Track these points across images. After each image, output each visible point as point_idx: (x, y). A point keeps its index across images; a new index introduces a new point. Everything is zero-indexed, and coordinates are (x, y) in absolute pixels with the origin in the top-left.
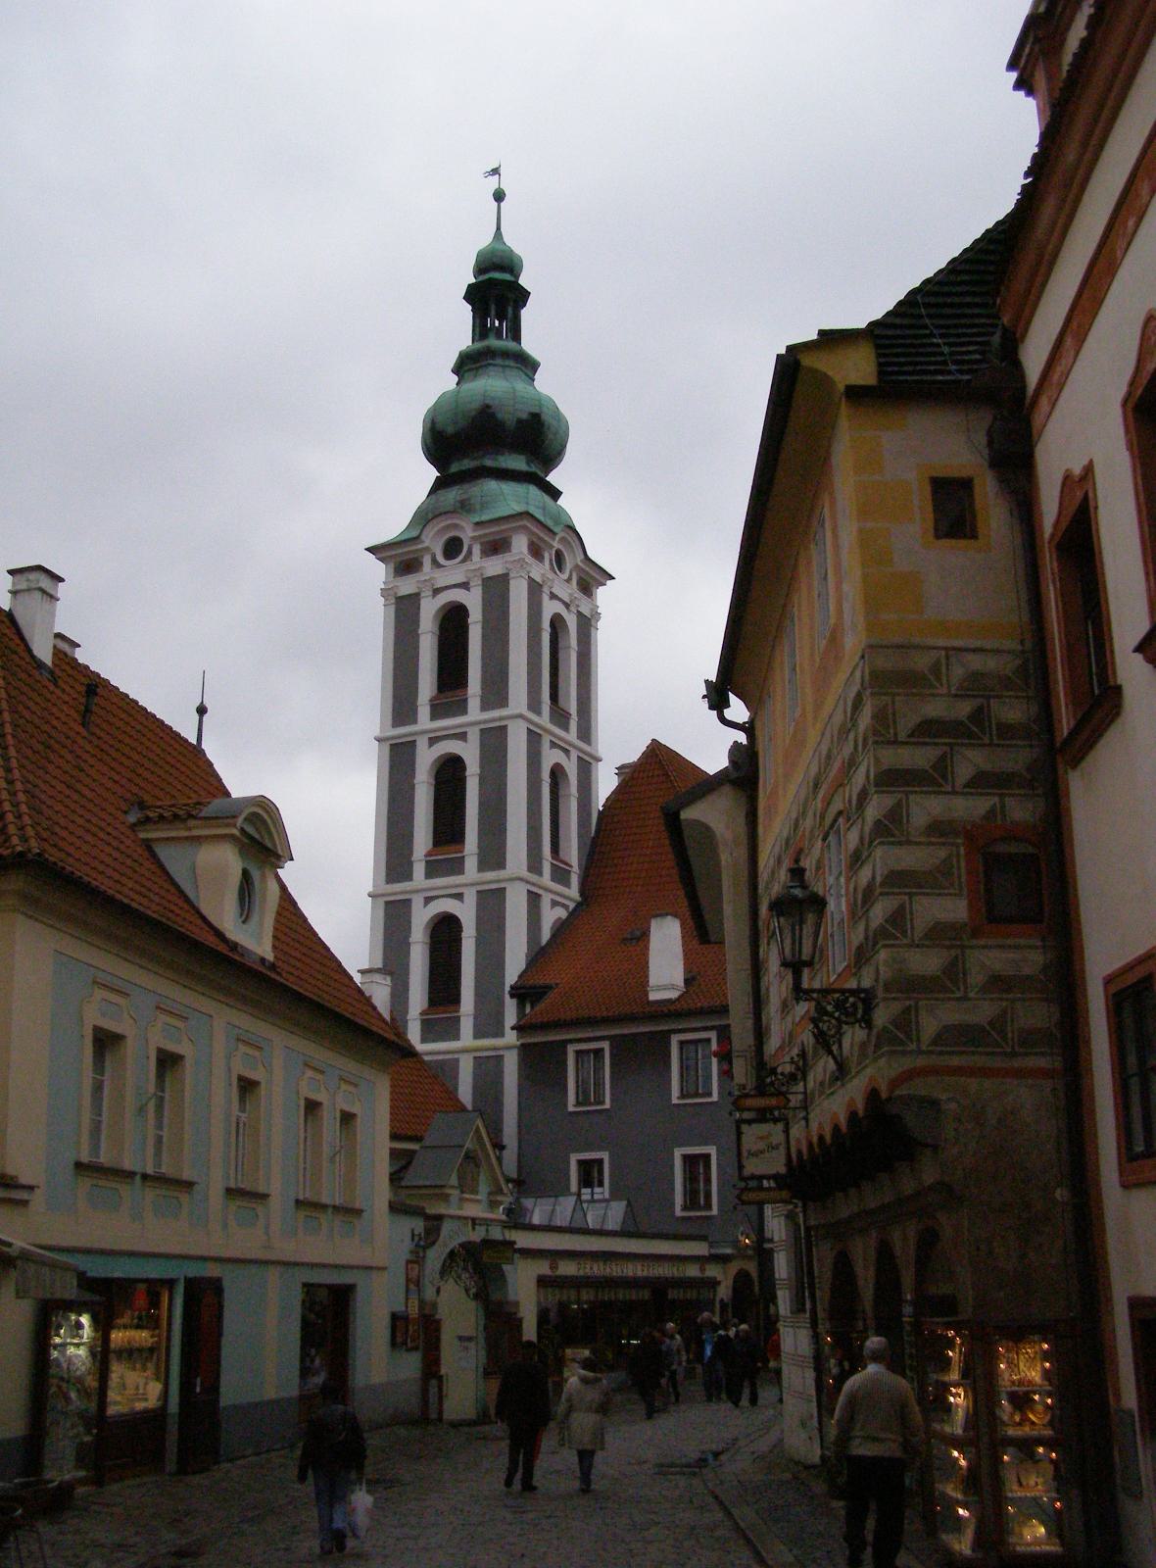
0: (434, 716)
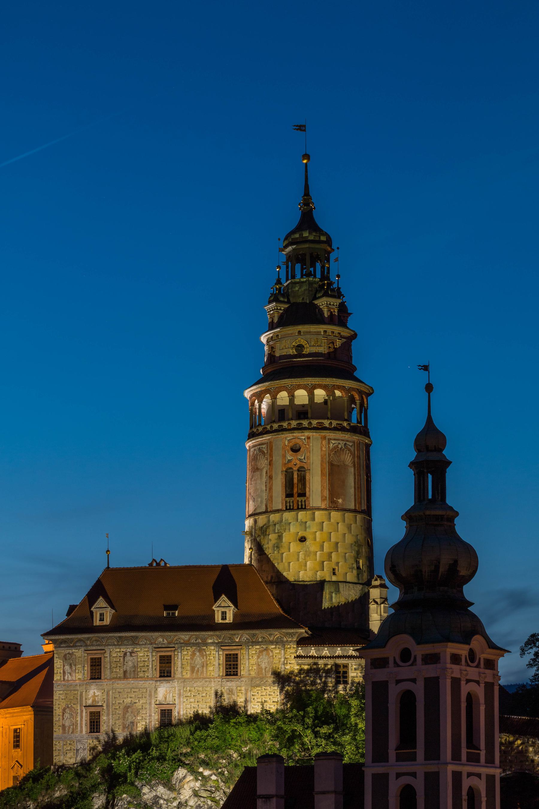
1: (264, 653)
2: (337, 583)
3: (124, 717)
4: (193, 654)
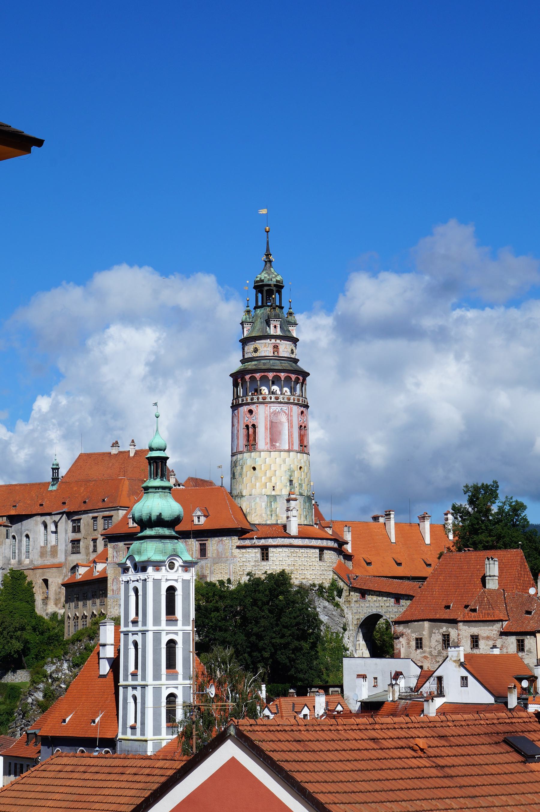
1: (221, 542)
2: (275, 496)
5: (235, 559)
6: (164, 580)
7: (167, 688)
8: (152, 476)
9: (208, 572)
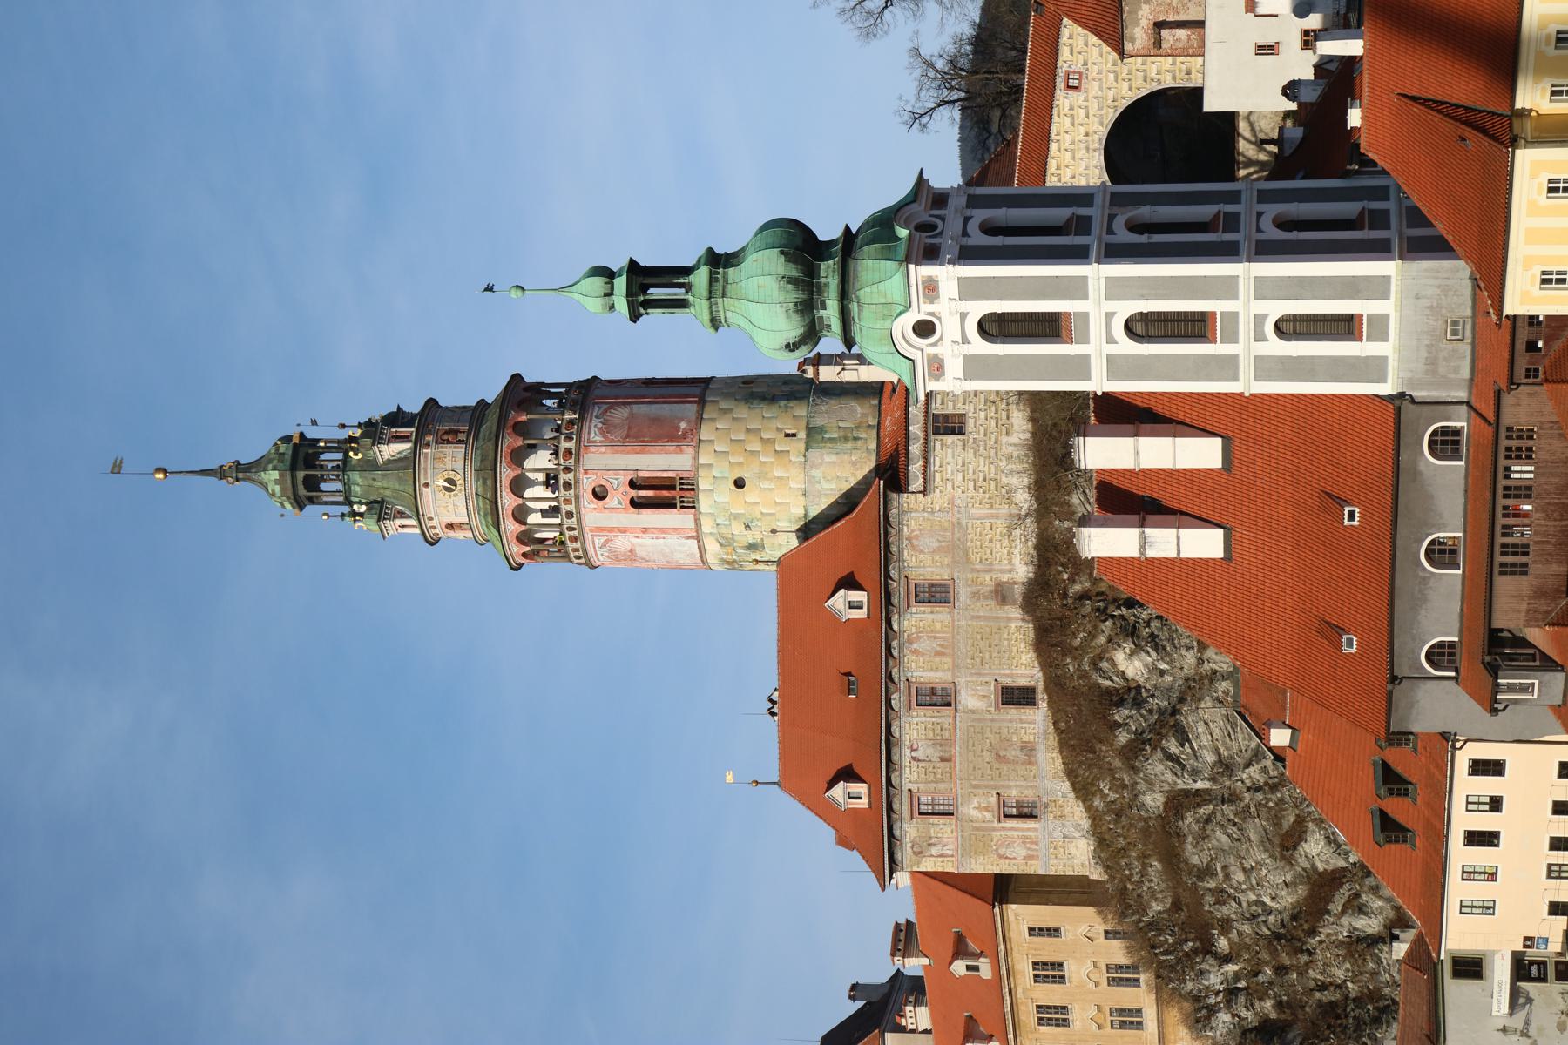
0: (1085, 340)
1: (915, 542)
3: (1015, 762)
4: (915, 652)
5: (958, 502)
6: (965, 241)
7: (1259, 230)
8: (678, 293)
9: (988, 577)
